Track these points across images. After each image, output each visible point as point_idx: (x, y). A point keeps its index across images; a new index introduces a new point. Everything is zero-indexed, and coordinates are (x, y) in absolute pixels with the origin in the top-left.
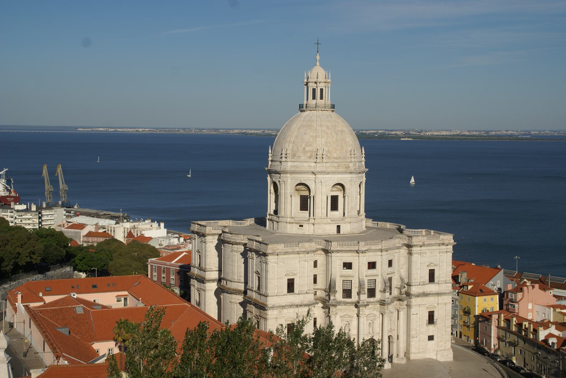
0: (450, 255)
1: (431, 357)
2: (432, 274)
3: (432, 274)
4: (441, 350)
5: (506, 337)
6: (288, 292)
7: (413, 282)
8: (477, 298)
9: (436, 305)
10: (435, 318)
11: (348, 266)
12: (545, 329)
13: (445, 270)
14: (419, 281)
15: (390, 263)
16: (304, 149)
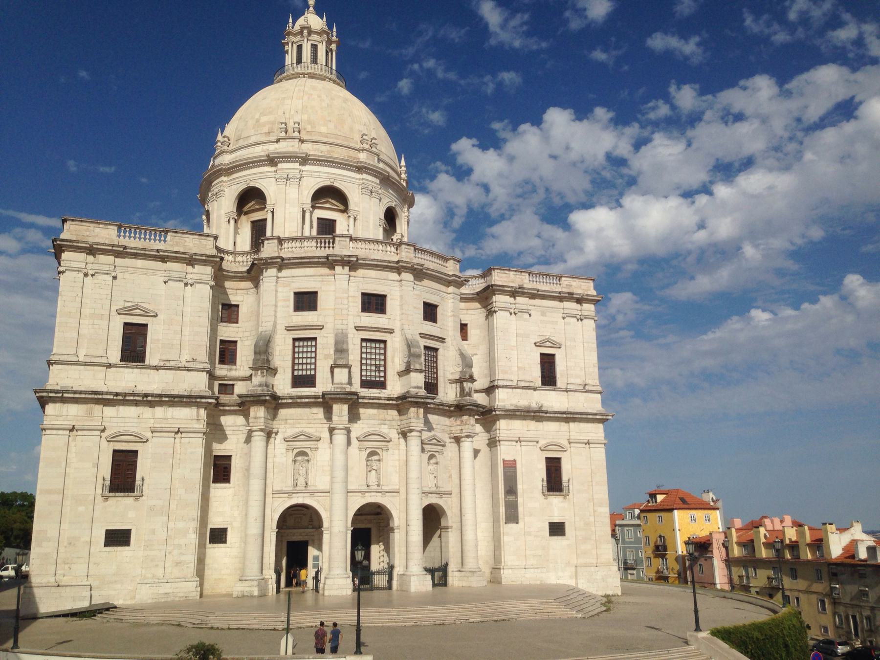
0: (590, 324)
1: (560, 582)
2: (548, 364)
3: (548, 364)
4: (586, 565)
5: (748, 577)
6: (122, 360)
7: (501, 377)
8: (675, 511)
9: (565, 443)
10: (565, 478)
11: (306, 301)
12: (842, 530)
13: (580, 360)
14: (515, 379)
15: (430, 312)
16: (258, 121)
